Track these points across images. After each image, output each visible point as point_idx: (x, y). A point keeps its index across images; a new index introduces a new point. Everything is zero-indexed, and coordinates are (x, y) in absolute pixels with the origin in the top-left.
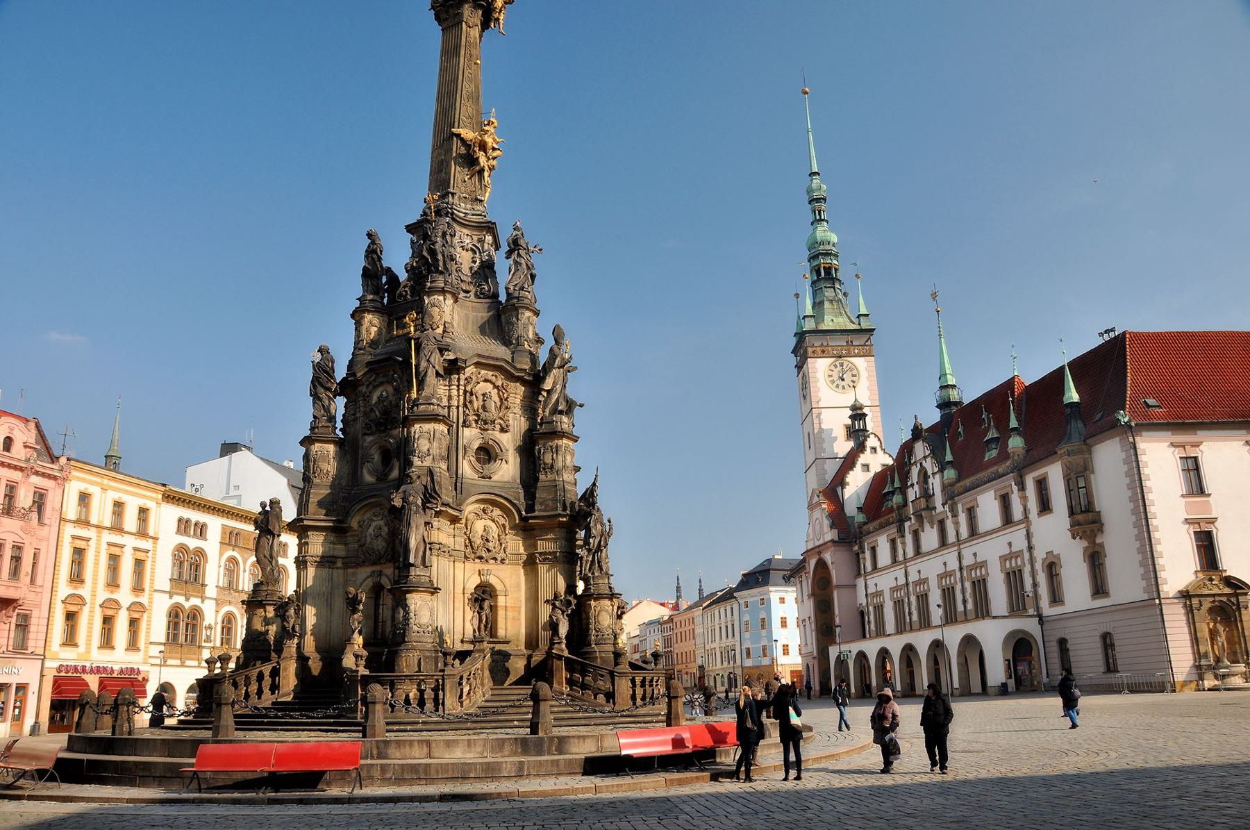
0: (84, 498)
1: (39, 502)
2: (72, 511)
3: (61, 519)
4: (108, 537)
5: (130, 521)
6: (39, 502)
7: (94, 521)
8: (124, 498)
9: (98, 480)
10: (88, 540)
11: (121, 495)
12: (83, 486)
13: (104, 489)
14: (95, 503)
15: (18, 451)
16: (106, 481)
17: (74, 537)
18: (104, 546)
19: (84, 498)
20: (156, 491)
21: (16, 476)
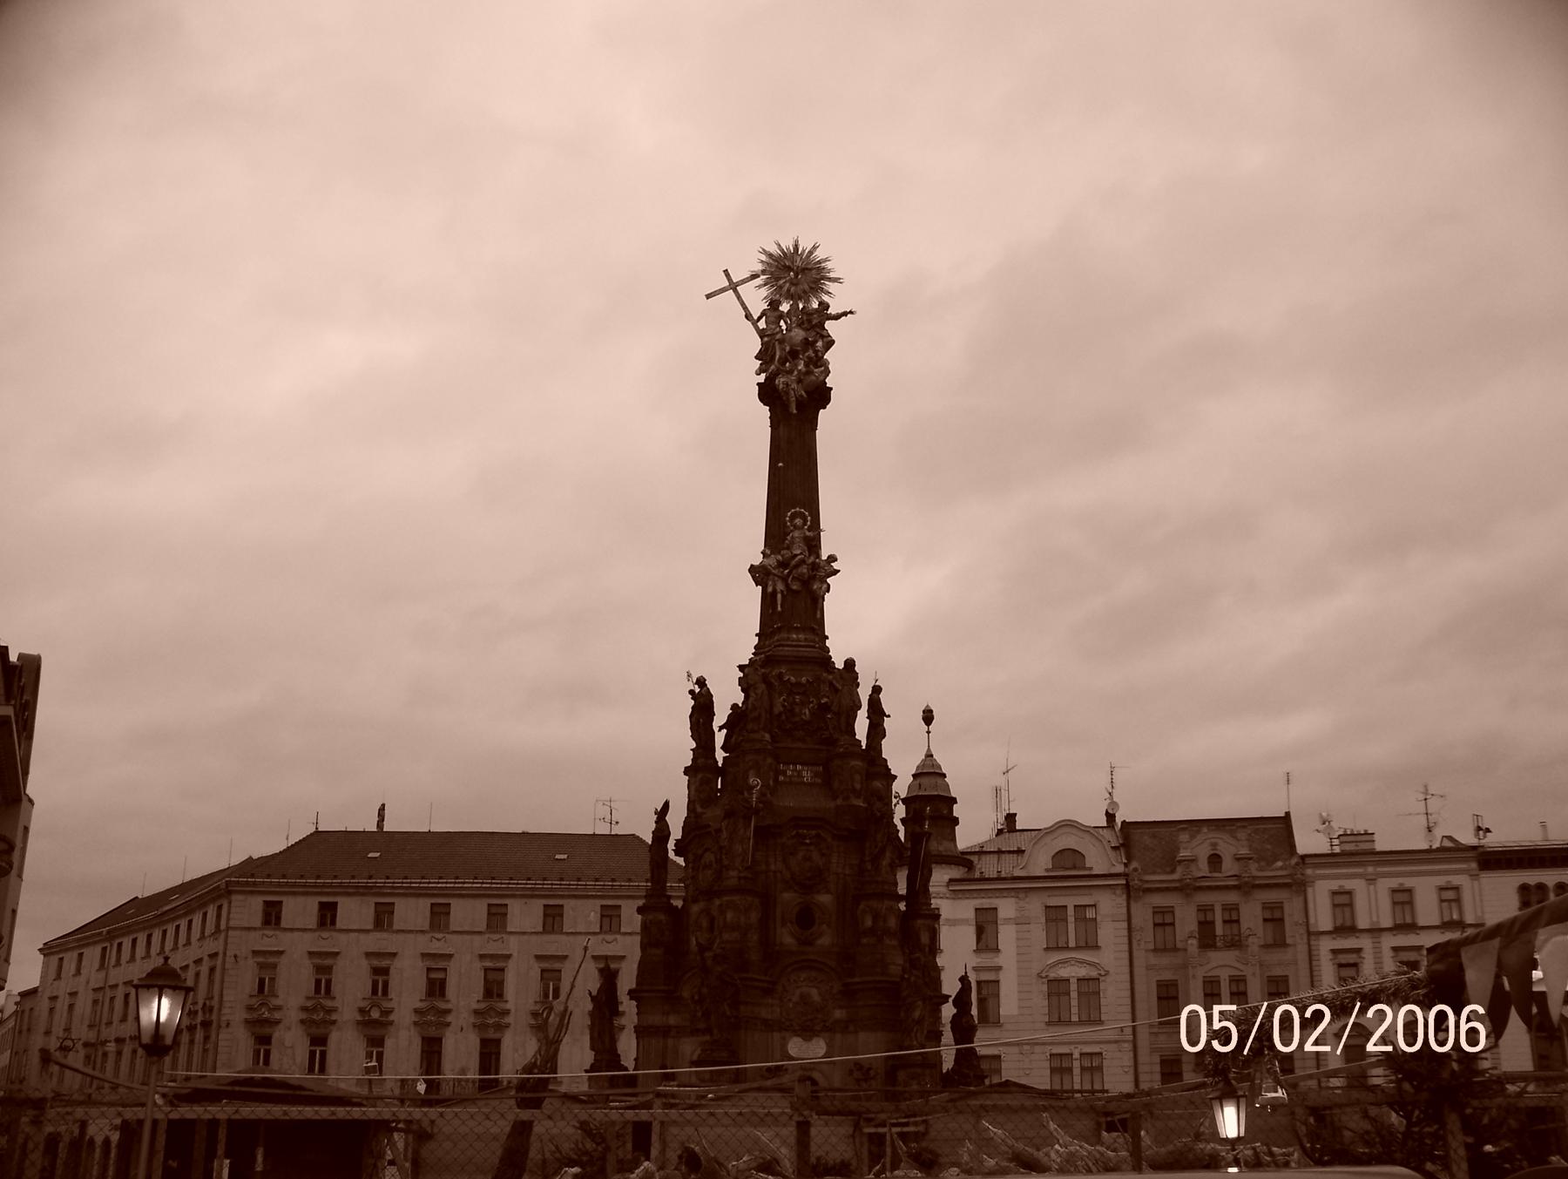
0: (1343, 901)
1: (1274, 919)
2: (1323, 918)
3: (1309, 933)
4: (1389, 941)
5: (1427, 910)
6: (1274, 919)
7: (1363, 922)
8: (1408, 882)
9: (1360, 870)
10: (1359, 951)
11: (1401, 880)
12: (1334, 885)
13: (1371, 880)
14: (1361, 903)
15: (1229, 867)
16: (1370, 869)
17: (1334, 952)
18: (1387, 955)
19: (1343, 901)
20: (1465, 860)
21: (1232, 897)
